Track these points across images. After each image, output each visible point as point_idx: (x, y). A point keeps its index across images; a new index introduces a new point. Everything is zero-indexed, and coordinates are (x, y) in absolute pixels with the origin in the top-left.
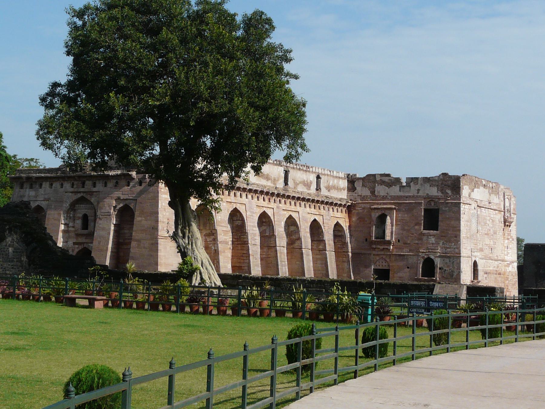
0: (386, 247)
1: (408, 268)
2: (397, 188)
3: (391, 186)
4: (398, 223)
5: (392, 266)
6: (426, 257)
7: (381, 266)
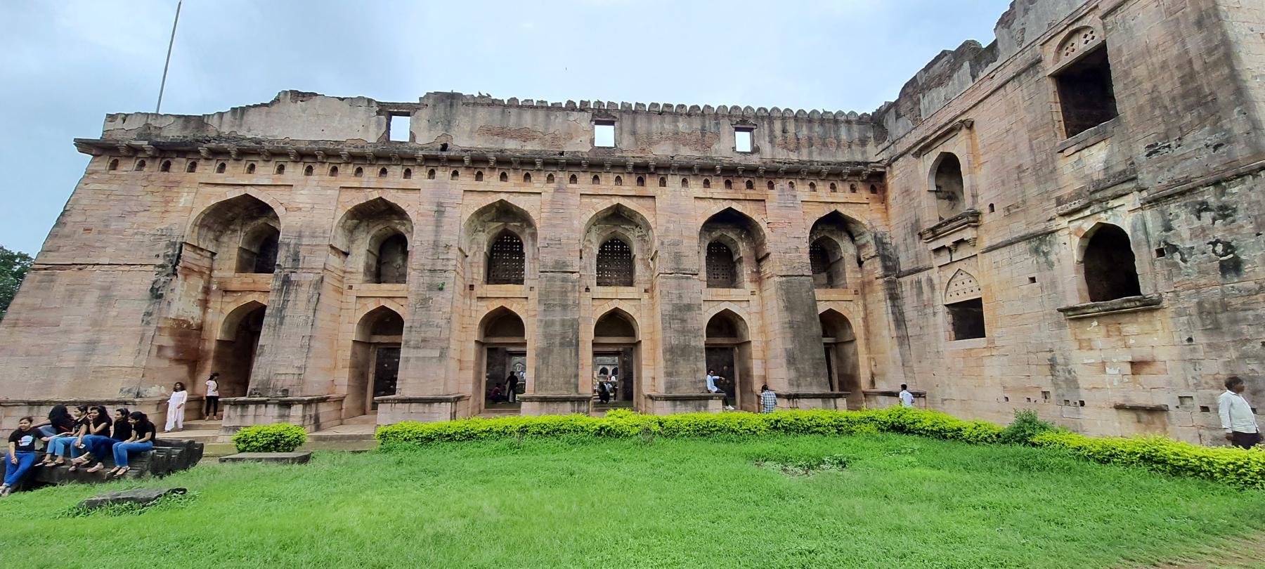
0: (956, 237)
1: (1033, 280)
2: (966, 65)
3: (950, 77)
4: (982, 159)
5: (988, 287)
6: (1088, 225)
7: (961, 293)
